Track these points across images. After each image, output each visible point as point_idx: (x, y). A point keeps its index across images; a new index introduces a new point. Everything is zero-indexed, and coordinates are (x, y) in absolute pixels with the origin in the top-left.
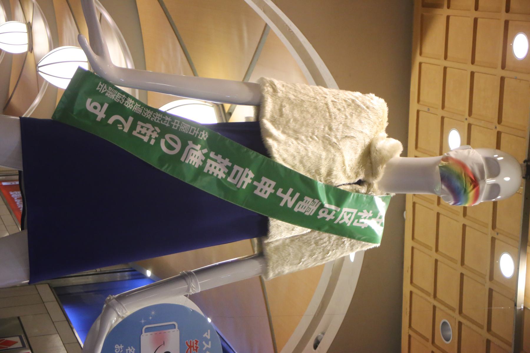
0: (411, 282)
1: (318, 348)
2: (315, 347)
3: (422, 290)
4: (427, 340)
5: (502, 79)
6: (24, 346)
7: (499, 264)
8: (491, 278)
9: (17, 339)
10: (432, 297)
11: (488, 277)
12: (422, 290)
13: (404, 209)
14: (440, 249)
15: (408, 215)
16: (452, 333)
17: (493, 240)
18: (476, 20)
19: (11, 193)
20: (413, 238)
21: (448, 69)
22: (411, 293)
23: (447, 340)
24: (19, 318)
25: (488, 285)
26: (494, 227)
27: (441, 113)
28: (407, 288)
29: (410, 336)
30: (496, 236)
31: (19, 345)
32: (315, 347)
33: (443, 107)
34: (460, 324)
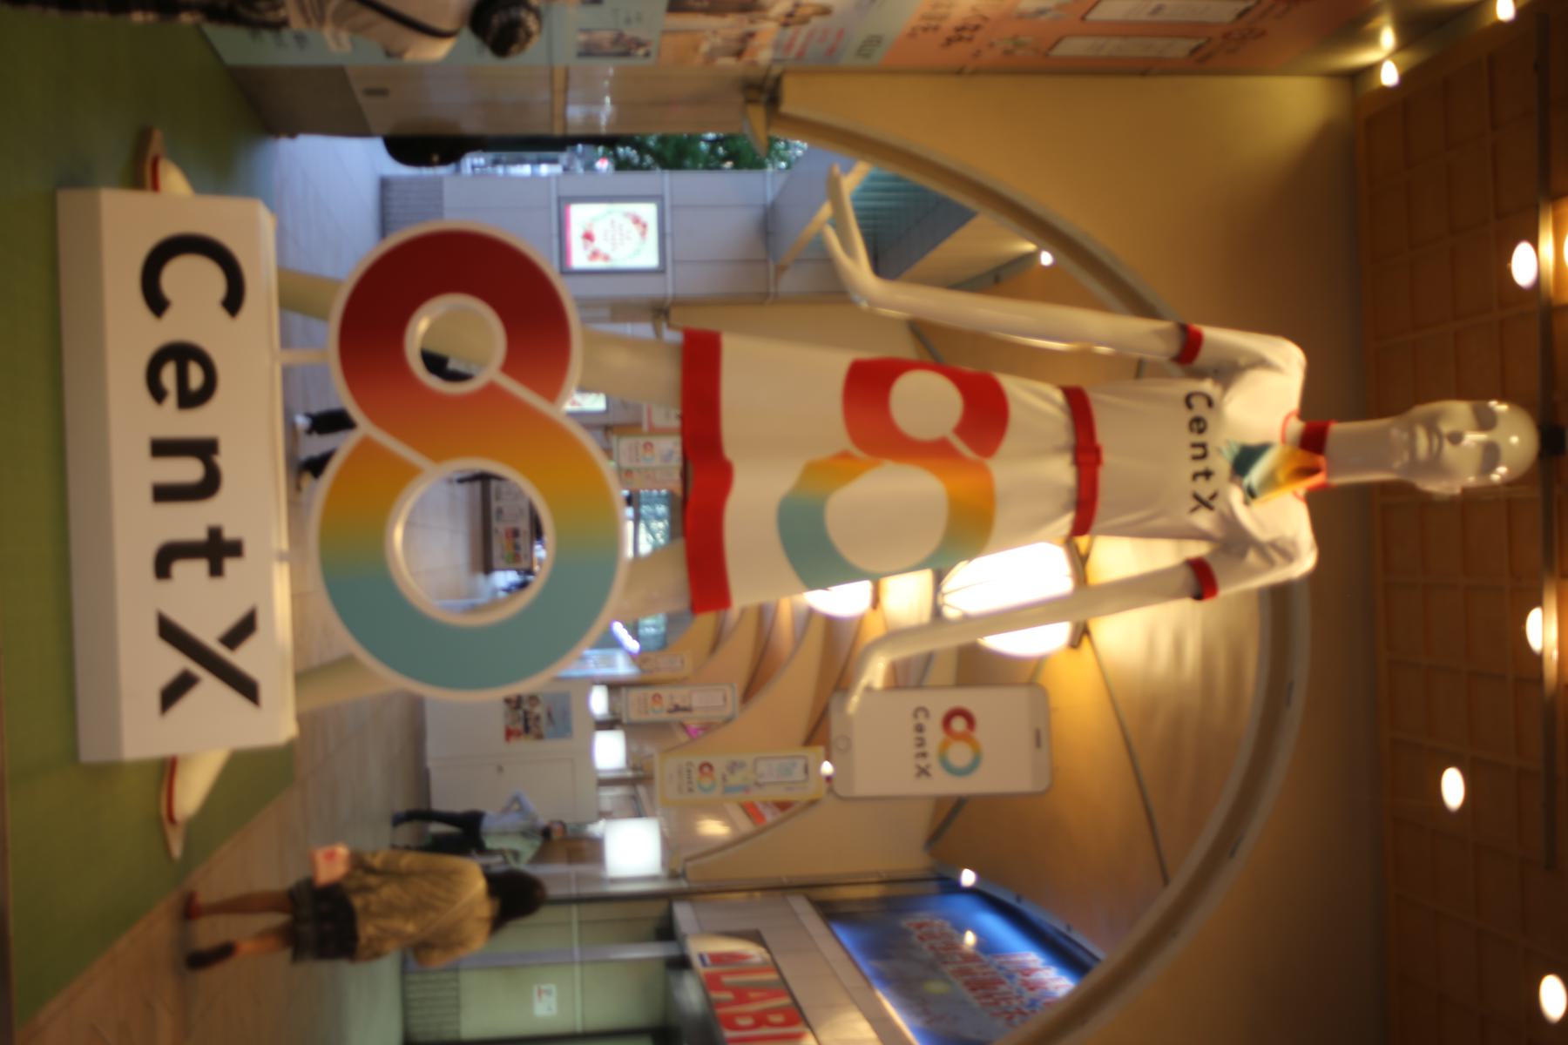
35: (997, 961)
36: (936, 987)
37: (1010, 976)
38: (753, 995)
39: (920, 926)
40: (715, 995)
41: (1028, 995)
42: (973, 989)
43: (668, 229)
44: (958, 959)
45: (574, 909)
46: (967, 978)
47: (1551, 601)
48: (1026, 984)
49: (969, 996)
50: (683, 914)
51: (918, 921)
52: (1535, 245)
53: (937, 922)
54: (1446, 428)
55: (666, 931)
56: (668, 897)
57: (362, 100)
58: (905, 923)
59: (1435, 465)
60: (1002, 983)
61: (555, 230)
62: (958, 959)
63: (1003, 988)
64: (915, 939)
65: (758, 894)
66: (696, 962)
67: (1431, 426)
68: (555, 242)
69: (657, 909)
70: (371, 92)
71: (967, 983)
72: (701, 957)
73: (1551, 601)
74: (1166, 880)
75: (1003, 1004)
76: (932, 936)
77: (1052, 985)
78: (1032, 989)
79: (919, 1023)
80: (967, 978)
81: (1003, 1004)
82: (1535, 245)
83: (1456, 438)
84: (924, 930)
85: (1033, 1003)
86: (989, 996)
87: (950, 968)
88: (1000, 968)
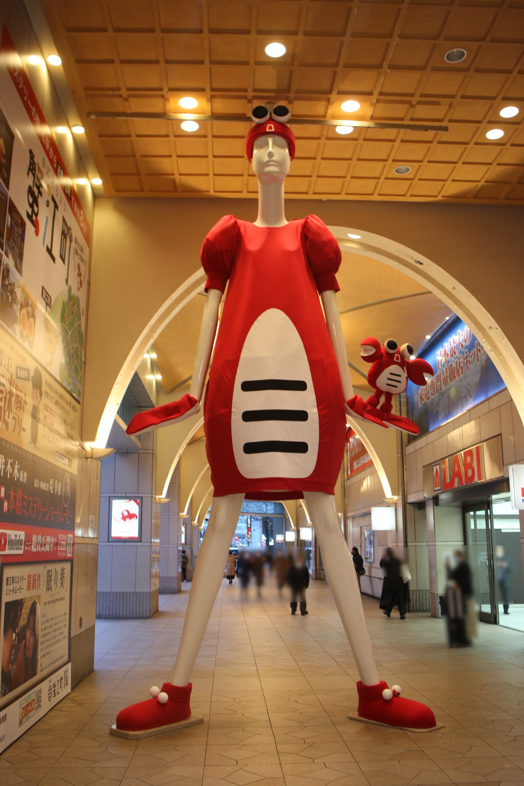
0: (372, 195)
1: (421, 262)
2: (422, 264)
3: (376, 187)
4: (411, 184)
5: (214, 137)
6: (439, 464)
7: (344, 135)
8: (356, 140)
9: (435, 468)
10: (379, 180)
11: (356, 142)
12: (376, 187)
13: (320, 201)
14: (343, 175)
15: (324, 198)
16: (403, 166)
17: (328, 139)
18: (178, 156)
19: (354, 469)
20: (339, 194)
21: (216, 173)
22: (379, 195)
23: (408, 170)
24: (423, 467)
25: (361, 142)
26: (319, 138)
27: (246, 177)
28: (376, 198)
29: (411, 196)
30: (325, 137)
31: (438, 467)
32: (422, 264)
33: (242, 175)
34: (394, 161)
35: (440, 367)
36: (453, 393)
37: (449, 362)
38: (456, 470)
39: (422, 399)
40: (456, 485)
41: (457, 354)
42: (455, 377)
43: (124, 495)
44: (439, 383)
45: (409, 544)
46: (448, 380)
47: (336, 122)
48: (452, 355)
49: (457, 378)
50: (412, 498)
51: (419, 399)
52: (183, 120)
53: (420, 392)
54: (266, 159)
55: (421, 505)
56: (405, 504)
57: (83, 629)
58: (420, 406)
59: (280, 164)
60: (451, 365)
61: (122, 544)
62: (439, 383)
63: (454, 365)
64: (428, 401)
65: (405, 467)
66: (434, 494)
67: (267, 164)
68: (126, 544)
69: (409, 508)
70: (81, 626)
71: (451, 380)
72: (435, 491)
73: (336, 122)
74: (430, 292)
75: (462, 365)
76: (427, 394)
77: (453, 345)
78: (455, 353)
79: (471, 400)
80: (448, 380)
81: (462, 365)
82: (183, 120)
83: (271, 155)
84: (423, 397)
85: (461, 352)
86: (458, 370)
87: (442, 387)
88: (444, 366)
